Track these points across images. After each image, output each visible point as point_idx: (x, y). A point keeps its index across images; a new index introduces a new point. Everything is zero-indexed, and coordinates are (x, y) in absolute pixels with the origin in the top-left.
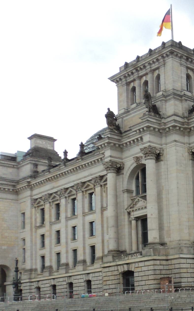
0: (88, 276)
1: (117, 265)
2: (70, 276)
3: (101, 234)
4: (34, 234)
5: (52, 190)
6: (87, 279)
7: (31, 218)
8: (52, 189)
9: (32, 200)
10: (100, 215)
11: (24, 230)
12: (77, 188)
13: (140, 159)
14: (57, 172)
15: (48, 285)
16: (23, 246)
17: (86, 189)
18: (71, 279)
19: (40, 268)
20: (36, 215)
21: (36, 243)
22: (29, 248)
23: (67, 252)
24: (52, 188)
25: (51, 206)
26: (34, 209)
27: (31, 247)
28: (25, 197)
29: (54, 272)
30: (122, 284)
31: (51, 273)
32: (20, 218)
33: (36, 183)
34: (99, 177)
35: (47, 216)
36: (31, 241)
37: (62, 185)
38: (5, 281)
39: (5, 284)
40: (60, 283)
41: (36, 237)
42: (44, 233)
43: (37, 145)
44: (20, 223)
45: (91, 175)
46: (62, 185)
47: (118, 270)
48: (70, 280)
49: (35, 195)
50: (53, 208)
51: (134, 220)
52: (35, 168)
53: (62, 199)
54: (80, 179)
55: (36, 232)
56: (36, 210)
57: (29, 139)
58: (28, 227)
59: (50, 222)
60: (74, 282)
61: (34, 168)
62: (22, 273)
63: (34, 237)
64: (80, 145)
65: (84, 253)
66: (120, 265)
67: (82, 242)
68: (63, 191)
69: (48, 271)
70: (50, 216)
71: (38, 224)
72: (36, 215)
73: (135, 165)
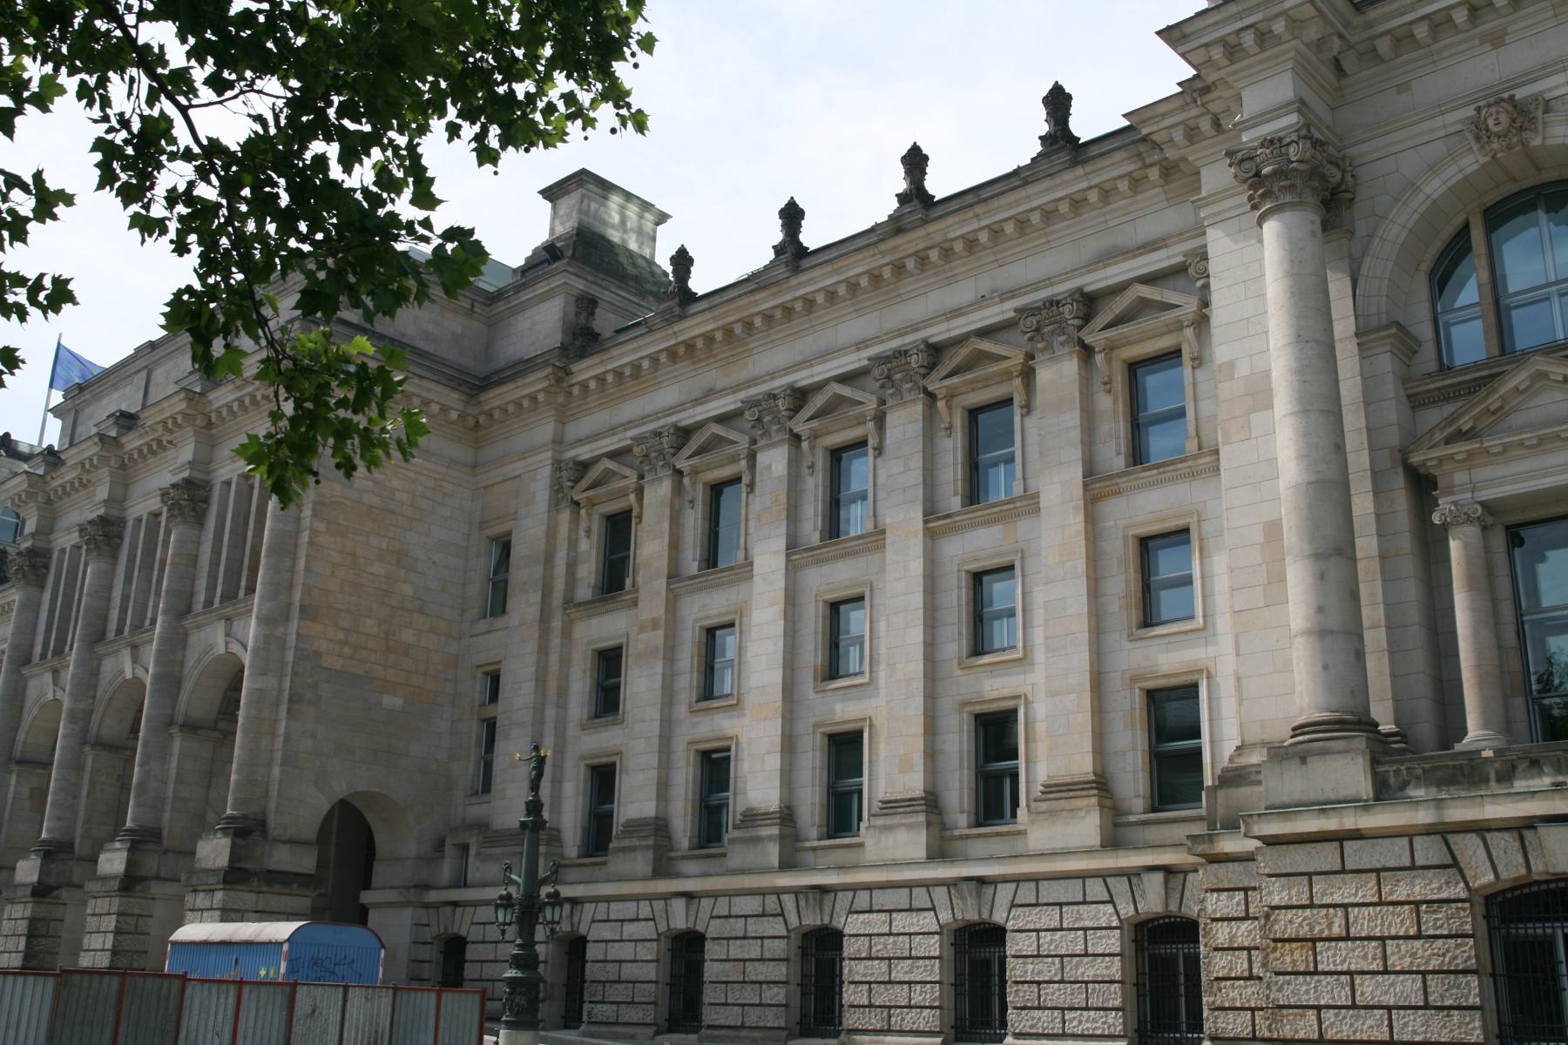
0: (979, 895)
1: (1443, 831)
2: (823, 890)
3: (1084, 637)
4: (555, 641)
5: (699, 409)
6: (972, 916)
7: (549, 559)
8: (698, 401)
9: (558, 465)
10: (1077, 522)
11: (500, 622)
12: (889, 377)
13: (1532, 120)
14: (756, 303)
15: (644, 930)
16: (482, 705)
17: (955, 380)
18: (827, 910)
19: (579, 831)
20: (573, 544)
21: (563, 692)
22: (526, 716)
23: (789, 745)
24: (697, 394)
25: (678, 489)
26: (565, 516)
27: (538, 710)
28: (523, 455)
29: (683, 858)
30: (1491, 980)
31: (663, 867)
32: (482, 565)
33: (600, 379)
34: (1077, 296)
35: (650, 548)
36: (541, 679)
37: (773, 375)
38: (367, 885)
39: (366, 897)
40: (737, 926)
41: (565, 662)
42: (624, 640)
43: (586, 219)
44: (477, 588)
45: (1005, 296)
46: (773, 375)
47: (1455, 864)
48: (821, 910)
49: (579, 442)
50: (692, 501)
51: (1469, 520)
52: (585, 314)
53: (763, 448)
54: (915, 328)
55: (567, 633)
56: (575, 518)
57: (545, 198)
58: (524, 606)
59: (674, 575)
60: (853, 925)
61: (577, 314)
62: (473, 850)
63: (554, 659)
64: (905, 160)
65: (932, 755)
66: (1481, 829)
67: (918, 685)
68: (780, 402)
69: (647, 847)
70: (675, 546)
71: (584, 592)
72: (573, 544)
73: (1475, 167)
